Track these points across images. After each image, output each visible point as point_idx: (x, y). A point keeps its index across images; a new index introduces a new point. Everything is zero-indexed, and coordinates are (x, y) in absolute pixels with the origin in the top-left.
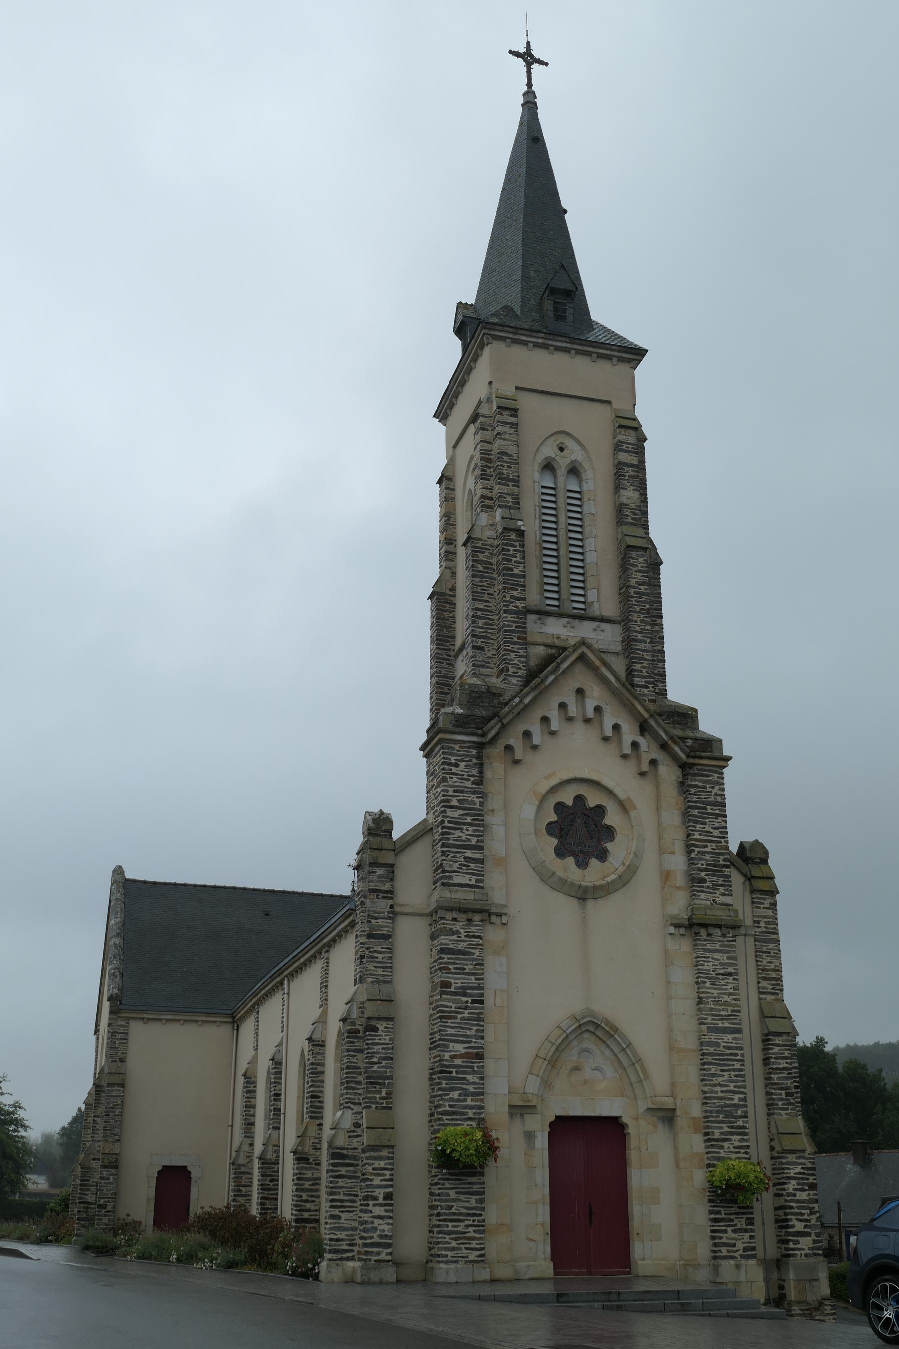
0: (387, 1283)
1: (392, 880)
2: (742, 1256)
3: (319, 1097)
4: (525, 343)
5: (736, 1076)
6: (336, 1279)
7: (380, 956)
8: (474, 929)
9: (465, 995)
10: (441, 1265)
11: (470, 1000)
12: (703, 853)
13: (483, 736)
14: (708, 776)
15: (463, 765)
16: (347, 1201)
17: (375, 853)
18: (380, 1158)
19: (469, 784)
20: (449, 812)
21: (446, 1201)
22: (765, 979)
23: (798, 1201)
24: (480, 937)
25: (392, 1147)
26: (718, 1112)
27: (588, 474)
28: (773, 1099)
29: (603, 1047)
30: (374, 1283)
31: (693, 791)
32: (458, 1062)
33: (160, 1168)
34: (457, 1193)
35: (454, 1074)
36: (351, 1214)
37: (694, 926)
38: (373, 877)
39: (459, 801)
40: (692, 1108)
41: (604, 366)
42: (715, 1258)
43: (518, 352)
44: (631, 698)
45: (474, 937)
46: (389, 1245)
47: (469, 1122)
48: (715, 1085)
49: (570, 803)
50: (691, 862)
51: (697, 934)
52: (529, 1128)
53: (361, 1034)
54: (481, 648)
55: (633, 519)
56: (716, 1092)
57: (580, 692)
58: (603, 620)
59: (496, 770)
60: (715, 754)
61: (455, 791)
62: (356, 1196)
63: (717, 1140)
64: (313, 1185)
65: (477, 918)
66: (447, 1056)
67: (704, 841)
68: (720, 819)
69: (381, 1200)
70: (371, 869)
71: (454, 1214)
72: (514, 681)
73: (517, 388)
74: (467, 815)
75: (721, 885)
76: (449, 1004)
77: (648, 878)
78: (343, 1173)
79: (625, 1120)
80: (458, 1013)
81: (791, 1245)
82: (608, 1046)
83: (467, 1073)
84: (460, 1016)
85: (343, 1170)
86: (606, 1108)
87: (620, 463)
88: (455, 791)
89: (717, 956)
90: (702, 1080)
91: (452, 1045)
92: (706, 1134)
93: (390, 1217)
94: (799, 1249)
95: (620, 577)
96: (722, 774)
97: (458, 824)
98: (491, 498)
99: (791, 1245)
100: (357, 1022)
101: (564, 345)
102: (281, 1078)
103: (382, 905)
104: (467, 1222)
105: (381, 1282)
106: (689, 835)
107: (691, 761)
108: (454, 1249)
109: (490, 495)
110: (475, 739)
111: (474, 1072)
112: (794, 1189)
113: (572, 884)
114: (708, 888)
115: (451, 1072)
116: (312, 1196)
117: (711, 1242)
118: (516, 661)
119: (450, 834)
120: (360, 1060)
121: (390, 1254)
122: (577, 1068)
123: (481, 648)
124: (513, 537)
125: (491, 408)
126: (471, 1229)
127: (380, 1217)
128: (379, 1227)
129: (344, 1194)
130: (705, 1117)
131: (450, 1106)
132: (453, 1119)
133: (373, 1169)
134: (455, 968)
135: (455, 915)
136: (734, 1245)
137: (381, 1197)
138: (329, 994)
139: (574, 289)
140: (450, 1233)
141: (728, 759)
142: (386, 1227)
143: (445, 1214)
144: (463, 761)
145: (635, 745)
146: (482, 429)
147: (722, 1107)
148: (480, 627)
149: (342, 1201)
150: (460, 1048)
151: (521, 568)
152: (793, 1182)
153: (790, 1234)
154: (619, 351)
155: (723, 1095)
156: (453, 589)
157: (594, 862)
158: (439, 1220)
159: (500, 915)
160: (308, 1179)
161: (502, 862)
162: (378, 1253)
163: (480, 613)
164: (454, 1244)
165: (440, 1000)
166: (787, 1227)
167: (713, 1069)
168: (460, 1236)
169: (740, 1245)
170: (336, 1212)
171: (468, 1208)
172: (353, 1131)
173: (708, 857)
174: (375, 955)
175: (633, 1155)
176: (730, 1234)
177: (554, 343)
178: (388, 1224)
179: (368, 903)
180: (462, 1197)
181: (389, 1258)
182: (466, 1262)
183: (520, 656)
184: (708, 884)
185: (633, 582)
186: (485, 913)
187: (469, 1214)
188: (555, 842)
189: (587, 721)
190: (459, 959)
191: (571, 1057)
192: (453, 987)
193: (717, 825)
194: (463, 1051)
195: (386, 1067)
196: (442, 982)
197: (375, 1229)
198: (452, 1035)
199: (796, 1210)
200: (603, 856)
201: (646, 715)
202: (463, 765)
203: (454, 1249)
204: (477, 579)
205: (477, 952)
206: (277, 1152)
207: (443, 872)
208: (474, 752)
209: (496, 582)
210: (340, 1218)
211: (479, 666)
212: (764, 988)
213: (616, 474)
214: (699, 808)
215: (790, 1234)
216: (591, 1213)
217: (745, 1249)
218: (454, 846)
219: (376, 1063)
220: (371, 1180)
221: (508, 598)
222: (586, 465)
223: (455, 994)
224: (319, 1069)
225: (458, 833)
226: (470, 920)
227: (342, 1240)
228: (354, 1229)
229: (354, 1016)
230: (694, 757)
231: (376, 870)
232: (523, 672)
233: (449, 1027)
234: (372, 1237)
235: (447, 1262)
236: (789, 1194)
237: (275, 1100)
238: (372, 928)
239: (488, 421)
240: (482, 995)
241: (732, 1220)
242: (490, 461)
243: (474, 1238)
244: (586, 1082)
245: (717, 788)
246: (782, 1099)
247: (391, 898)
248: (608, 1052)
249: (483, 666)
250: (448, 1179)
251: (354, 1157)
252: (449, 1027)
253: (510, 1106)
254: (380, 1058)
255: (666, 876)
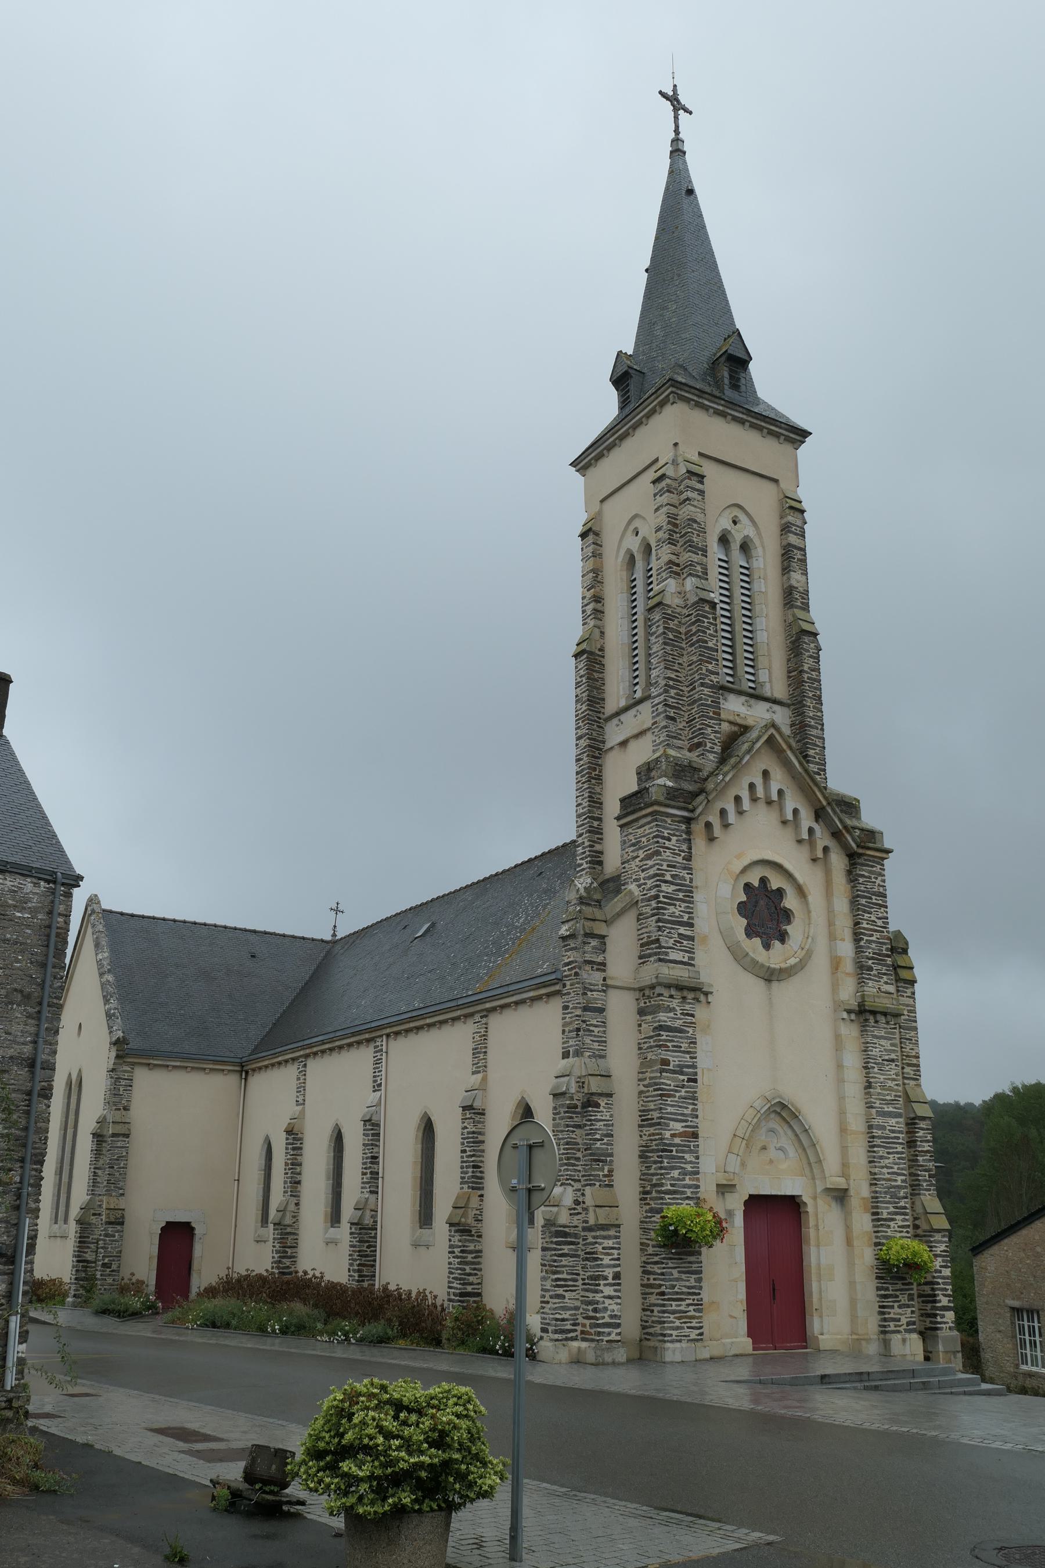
0: (620, 1364)
1: (604, 951)
2: (906, 1331)
3: (480, 1167)
4: (706, 408)
5: (899, 1158)
6: (564, 1360)
7: (596, 1030)
8: (687, 1007)
9: (682, 1073)
10: (668, 1345)
11: (686, 1078)
12: (870, 942)
13: (692, 811)
14: (873, 866)
15: (674, 838)
16: (570, 1280)
17: (588, 924)
18: (608, 1238)
19: (679, 859)
20: (664, 887)
21: (671, 1280)
22: (909, 1065)
23: (943, 1278)
24: (693, 1016)
25: (618, 1226)
26: (885, 1193)
27: (758, 552)
28: (919, 1180)
29: (786, 1127)
30: (608, 1364)
31: (861, 880)
32: (677, 1140)
33: (164, 1224)
34: (679, 1272)
35: (674, 1153)
36: (574, 1293)
37: (864, 1013)
38: (588, 948)
39: (672, 876)
40: (860, 1189)
41: (771, 443)
42: (884, 1332)
43: (698, 417)
44: (811, 784)
45: (687, 1014)
46: (618, 1325)
47: (687, 1202)
48: (883, 1167)
49: (756, 884)
50: (859, 950)
51: (866, 1020)
52: (729, 1207)
53: (579, 1110)
54: (673, 719)
55: (802, 603)
56: (884, 1174)
57: (766, 774)
58: (775, 702)
59: (699, 843)
60: (878, 845)
61: (668, 866)
62: (578, 1274)
63: (885, 1220)
64: (475, 1257)
65: (690, 996)
66: (667, 1134)
67: (871, 930)
68: (883, 909)
69: (610, 1281)
70: (585, 940)
71: (677, 1293)
72: (711, 756)
73: (700, 454)
74: (679, 890)
75: (885, 974)
76: (668, 1082)
77: (820, 963)
78: (566, 1251)
79: (805, 1199)
80: (676, 1091)
81: (939, 1319)
82: (791, 1127)
83: (683, 1152)
84: (678, 1094)
85: (566, 1249)
86: (788, 1187)
87: (789, 545)
88: (668, 866)
89: (883, 1042)
90: (870, 1162)
91: (672, 1123)
92: (874, 1214)
93: (619, 1297)
94: (945, 1323)
95: (789, 660)
96: (883, 865)
97: (672, 900)
98: (678, 565)
99: (939, 1319)
100: (575, 1097)
101: (741, 415)
102: (379, 1140)
103: (596, 977)
104: (688, 1302)
105: (614, 1363)
106: (857, 924)
107: (861, 851)
108: (678, 1328)
109: (677, 561)
110: (685, 814)
111: (691, 1152)
112: (941, 1266)
113: (762, 966)
114: (875, 976)
115: (671, 1151)
116: (475, 1269)
117: (879, 1317)
118: (712, 737)
119: (665, 909)
120: (579, 1136)
121: (619, 1334)
122: (764, 1148)
123: (673, 719)
124: (707, 609)
125: (676, 471)
126: (691, 1308)
127: (610, 1297)
128: (610, 1307)
129: (568, 1274)
130: (873, 1198)
131: (672, 1185)
132: (674, 1199)
133: (603, 1248)
134: (674, 1046)
135: (673, 992)
136: (899, 1320)
137: (610, 1276)
138: (489, 1061)
139: (746, 358)
140: (674, 1312)
141: (888, 851)
142: (615, 1307)
143: (669, 1293)
144: (674, 835)
145: (811, 831)
146: (669, 491)
147: (889, 1188)
148: (672, 697)
149: (565, 1280)
150: (678, 1127)
151: (714, 642)
152: (940, 1259)
153: (938, 1308)
154: (786, 430)
155: (889, 1176)
156: (602, 649)
157: (777, 943)
158: (664, 1300)
159: (706, 994)
160: (471, 1252)
161: (705, 939)
162: (609, 1334)
163: (671, 683)
164: (678, 1323)
165: (660, 1078)
166: (935, 1302)
167: (881, 1152)
168: (682, 1315)
169: (904, 1321)
170: (560, 1291)
171: (689, 1287)
172: (574, 1209)
173: (873, 946)
174: (591, 1028)
175: (811, 1233)
176: (897, 1310)
177: (733, 413)
178: (617, 1304)
179: (584, 975)
180: (683, 1276)
181: (618, 1338)
182: (688, 1341)
183: (716, 732)
184: (874, 972)
185: (806, 668)
186: (694, 991)
187: (689, 1294)
188: (745, 922)
189: (769, 803)
190: (675, 1037)
191: (762, 1137)
192: (672, 1064)
193: (880, 915)
194: (682, 1130)
195: (607, 1144)
196: (662, 1059)
197: (606, 1309)
198: (671, 1113)
199: (942, 1286)
200: (783, 937)
201: (824, 803)
202: (674, 838)
203: (678, 1328)
204: (668, 648)
205: (690, 1030)
206: (374, 1217)
207: (660, 947)
208: (684, 827)
209: (685, 652)
210: (564, 1297)
211: (673, 737)
212: (908, 1073)
213: (783, 555)
214: (866, 897)
215: (938, 1308)
216: (774, 1289)
217: (908, 1324)
218: (669, 922)
219: (599, 1140)
220: (601, 1260)
221: (704, 671)
222: (757, 541)
223: (674, 1072)
224: (480, 1138)
225: (672, 909)
226: (684, 998)
227: (567, 1320)
228: (577, 1308)
229: (573, 1090)
230: (863, 847)
231: (590, 940)
232: (718, 749)
233: (669, 1105)
234: (604, 1318)
235: (672, 1342)
236: (936, 1271)
237: (371, 1163)
238: (588, 1002)
239: (675, 484)
240: (696, 1074)
241: (897, 1296)
242: (675, 525)
243: (693, 1317)
244: (771, 1161)
245: (880, 878)
246: (926, 1181)
247: (604, 971)
248: (789, 1132)
249: (675, 738)
250: (671, 1259)
251: (576, 1236)
252: (669, 1105)
253: (717, 1185)
254: (602, 1135)
255: (836, 964)
